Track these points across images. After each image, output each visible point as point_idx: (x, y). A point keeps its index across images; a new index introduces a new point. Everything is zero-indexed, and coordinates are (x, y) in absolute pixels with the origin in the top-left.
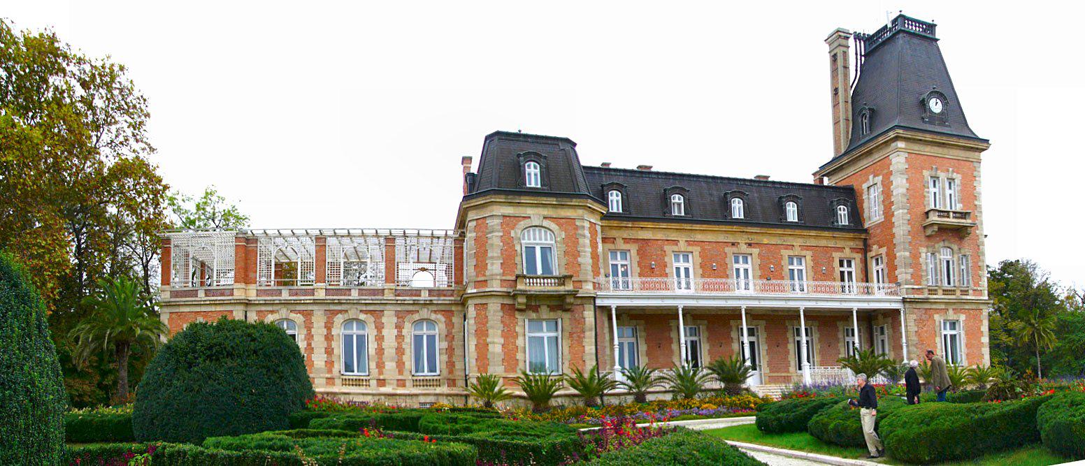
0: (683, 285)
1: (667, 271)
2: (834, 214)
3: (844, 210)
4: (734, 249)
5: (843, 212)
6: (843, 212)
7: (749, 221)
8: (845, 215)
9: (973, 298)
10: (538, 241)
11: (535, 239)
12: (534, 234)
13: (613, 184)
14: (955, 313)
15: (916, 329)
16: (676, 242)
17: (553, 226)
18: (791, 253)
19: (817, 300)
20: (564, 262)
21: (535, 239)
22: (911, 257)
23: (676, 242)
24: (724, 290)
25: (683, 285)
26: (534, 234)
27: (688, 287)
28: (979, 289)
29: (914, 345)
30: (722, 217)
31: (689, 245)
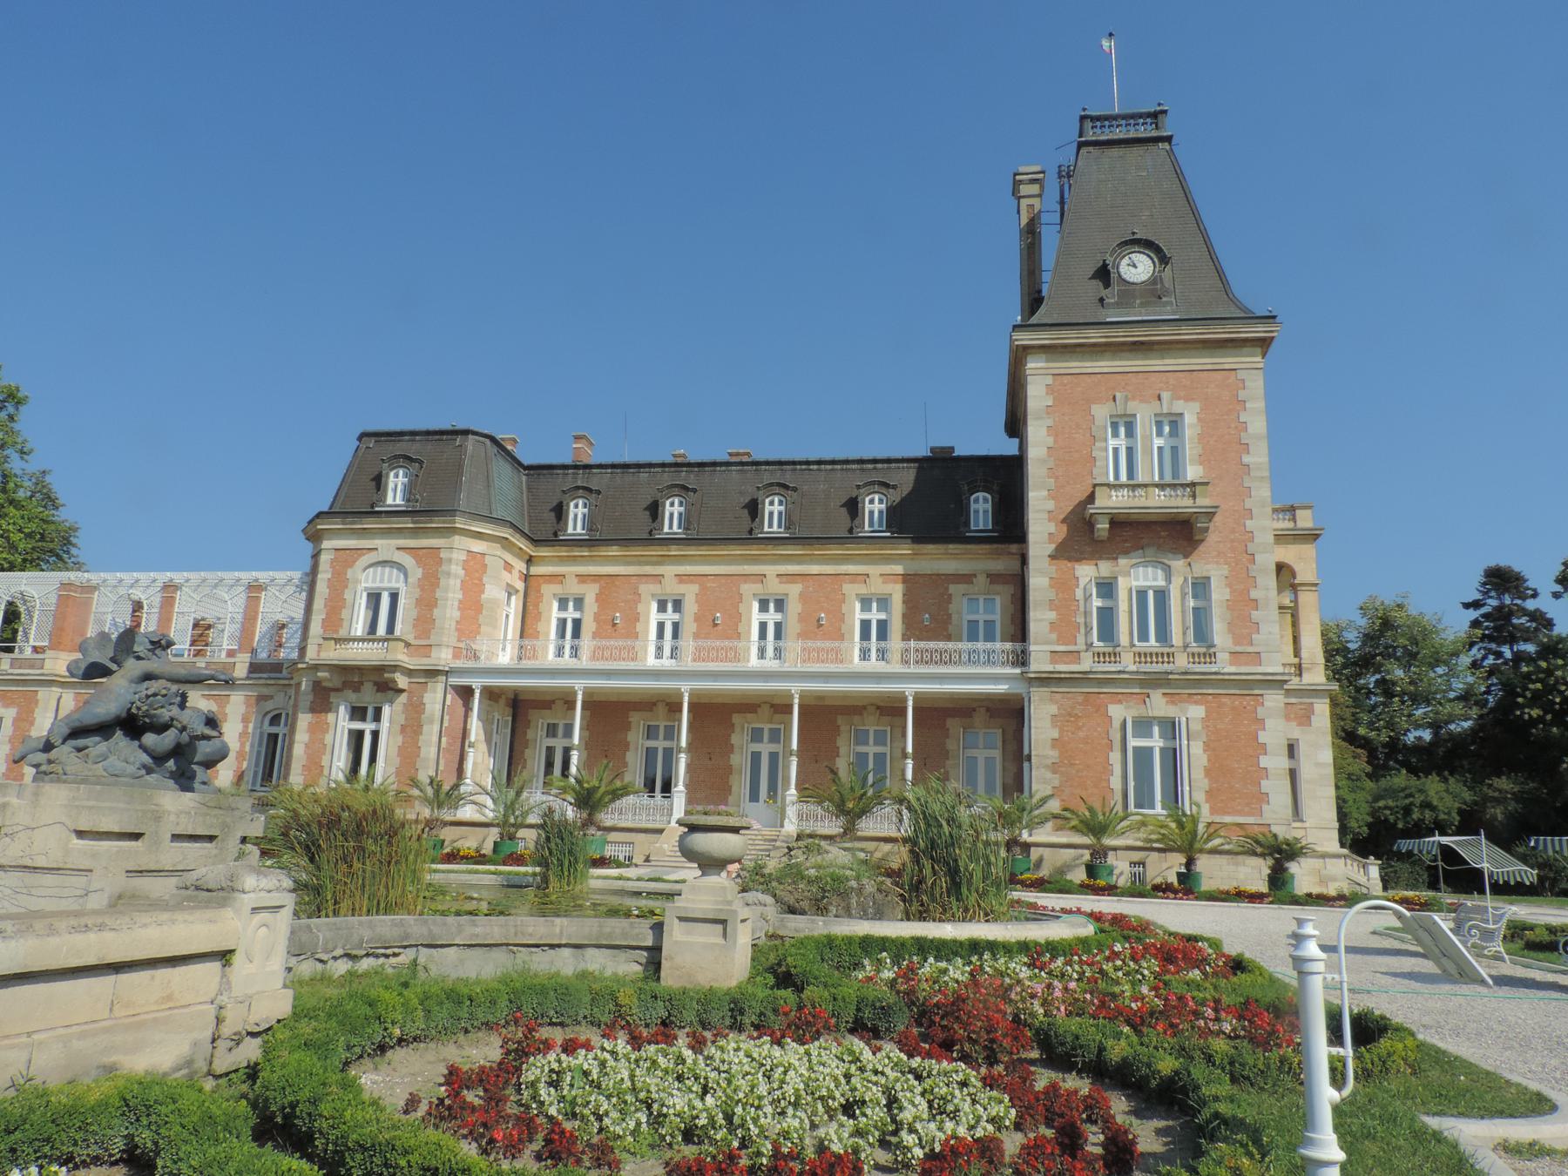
0: (667, 651)
1: (639, 627)
2: (963, 510)
3: (985, 500)
4: (757, 588)
5: (981, 507)
6: (981, 507)
7: (800, 537)
8: (985, 512)
9: (1233, 669)
10: (386, 585)
11: (382, 581)
12: (383, 574)
13: (578, 488)
14: (1173, 703)
15: (1056, 735)
16: (658, 578)
17: (407, 560)
18: (862, 590)
19: (608, 674)
20: (414, 614)
21: (382, 581)
22: (1051, 586)
23: (658, 578)
24: (726, 659)
25: (667, 651)
26: (383, 574)
27: (575, 651)
28: (1250, 649)
29: (1047, 767)
30: (743, 529)
31: (681, 582)
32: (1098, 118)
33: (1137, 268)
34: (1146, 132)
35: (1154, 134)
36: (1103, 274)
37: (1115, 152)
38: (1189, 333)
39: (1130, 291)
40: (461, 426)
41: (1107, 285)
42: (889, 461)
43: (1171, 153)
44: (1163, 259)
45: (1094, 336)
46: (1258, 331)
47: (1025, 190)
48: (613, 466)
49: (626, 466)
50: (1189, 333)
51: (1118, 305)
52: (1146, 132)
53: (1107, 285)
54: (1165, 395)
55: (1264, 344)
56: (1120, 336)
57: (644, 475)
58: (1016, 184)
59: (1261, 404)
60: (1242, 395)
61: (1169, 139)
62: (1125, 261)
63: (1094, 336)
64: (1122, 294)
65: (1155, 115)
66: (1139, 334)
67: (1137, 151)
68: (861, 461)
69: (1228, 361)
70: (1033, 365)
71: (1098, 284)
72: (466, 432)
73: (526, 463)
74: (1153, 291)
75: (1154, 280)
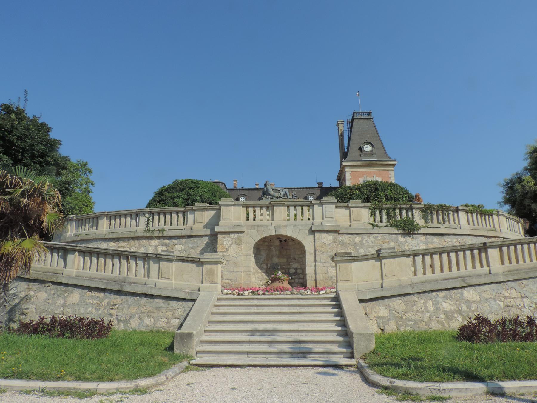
32: (358, 113)
33: (367, 148)
34: (368, 116)
35: (369, 117)
36: (360, 149)
37: (361, 121)
38: (379, 163)
39: (366, 153)
40: (216, 180)
41: (361, 152)
42: (313, 188)
43: (373, 121)
44: (373, 146)
45: (360, 163)
46: (393, 163)
47: (340, 125)
48: (249, 189)
49: (252, 189)
50: (379, 163)
51: (364, 156)
52: (368, 116)
53: (361, 152)
54: (374, 176)
55: (394, 165)
56: (365, 163)
57: (256, 191)
58: (337, 125)
59: (394, 178)
60: (390, 176)
61: (372, 118)
62: (366, 146)
63: (360, 163)
64: (364, 154)
65: (369, 113)
66: (369, 163)
67: (366, 121)
68: (307, 188)
69: (387, 169)
70: (347, 169)
71: (359, 151)
72: (219, 183)
73: (228, 188)
74: (371, 153)
75: (371, 151)
